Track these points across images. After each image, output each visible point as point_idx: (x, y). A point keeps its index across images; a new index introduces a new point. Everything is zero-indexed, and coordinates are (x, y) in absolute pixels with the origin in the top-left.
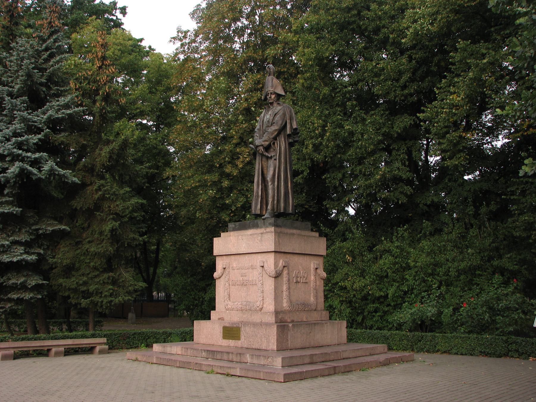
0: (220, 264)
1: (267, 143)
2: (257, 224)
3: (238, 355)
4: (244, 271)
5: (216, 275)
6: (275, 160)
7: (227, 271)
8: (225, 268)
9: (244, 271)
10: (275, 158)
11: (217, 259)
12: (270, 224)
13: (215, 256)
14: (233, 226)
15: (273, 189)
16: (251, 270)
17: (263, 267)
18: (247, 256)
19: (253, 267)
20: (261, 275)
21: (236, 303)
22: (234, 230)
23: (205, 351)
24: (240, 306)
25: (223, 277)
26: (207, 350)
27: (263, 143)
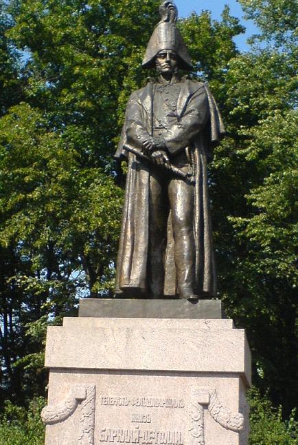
0: (60, 392)
1: (179, 146)
4: (141, 411)
5: (47, 412)
6: (194, 184)
7: (85, 408)
8: (79, 401)
9: (141, 411)
10: (192, 179)
11: (51, 375)
13: (46, 372)
15: (192, 240)
16: (165, 411)
17: (205, 406)
19: (170, 404)
20: (201, 422)
27: (168, 145)
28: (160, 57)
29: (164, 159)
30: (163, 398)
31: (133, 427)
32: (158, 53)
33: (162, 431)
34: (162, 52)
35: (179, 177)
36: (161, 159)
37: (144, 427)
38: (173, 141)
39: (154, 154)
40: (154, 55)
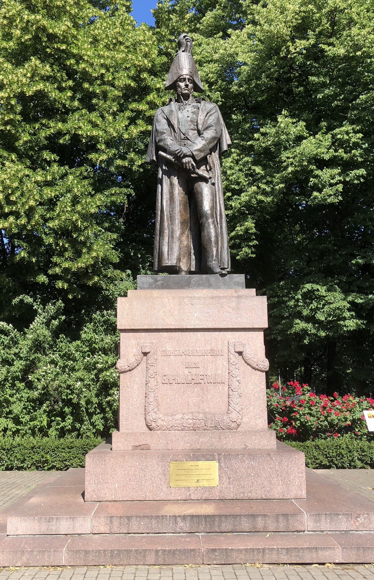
1: (202, 155)
2: (209, 281)
3: (281, 519)
4: (193, 359)
6: (213, 184)
8: (145, 354)
9: (193, 359)
12: (238, 284)
14: (151, 280)
16: (210, 358)
17: (240, 353)
18: (199, 334)
21: (179, 416)
22: (151, 287)
23: (184, 517)
24: (191, 421)
25: (139, 368)
26: (192, 517)
27: (195, 153)
28: (180, 81)
29: (192, 165)
30: (209, 348)
31: (186, 371)
32: (178, 78)
33: (209, 374)
34: (182, 77)
35: (205, 180)
36: (190, 165)
37: (194, 371)
38: (200, 150)
39: (184, 160)
40: (175, 79)
